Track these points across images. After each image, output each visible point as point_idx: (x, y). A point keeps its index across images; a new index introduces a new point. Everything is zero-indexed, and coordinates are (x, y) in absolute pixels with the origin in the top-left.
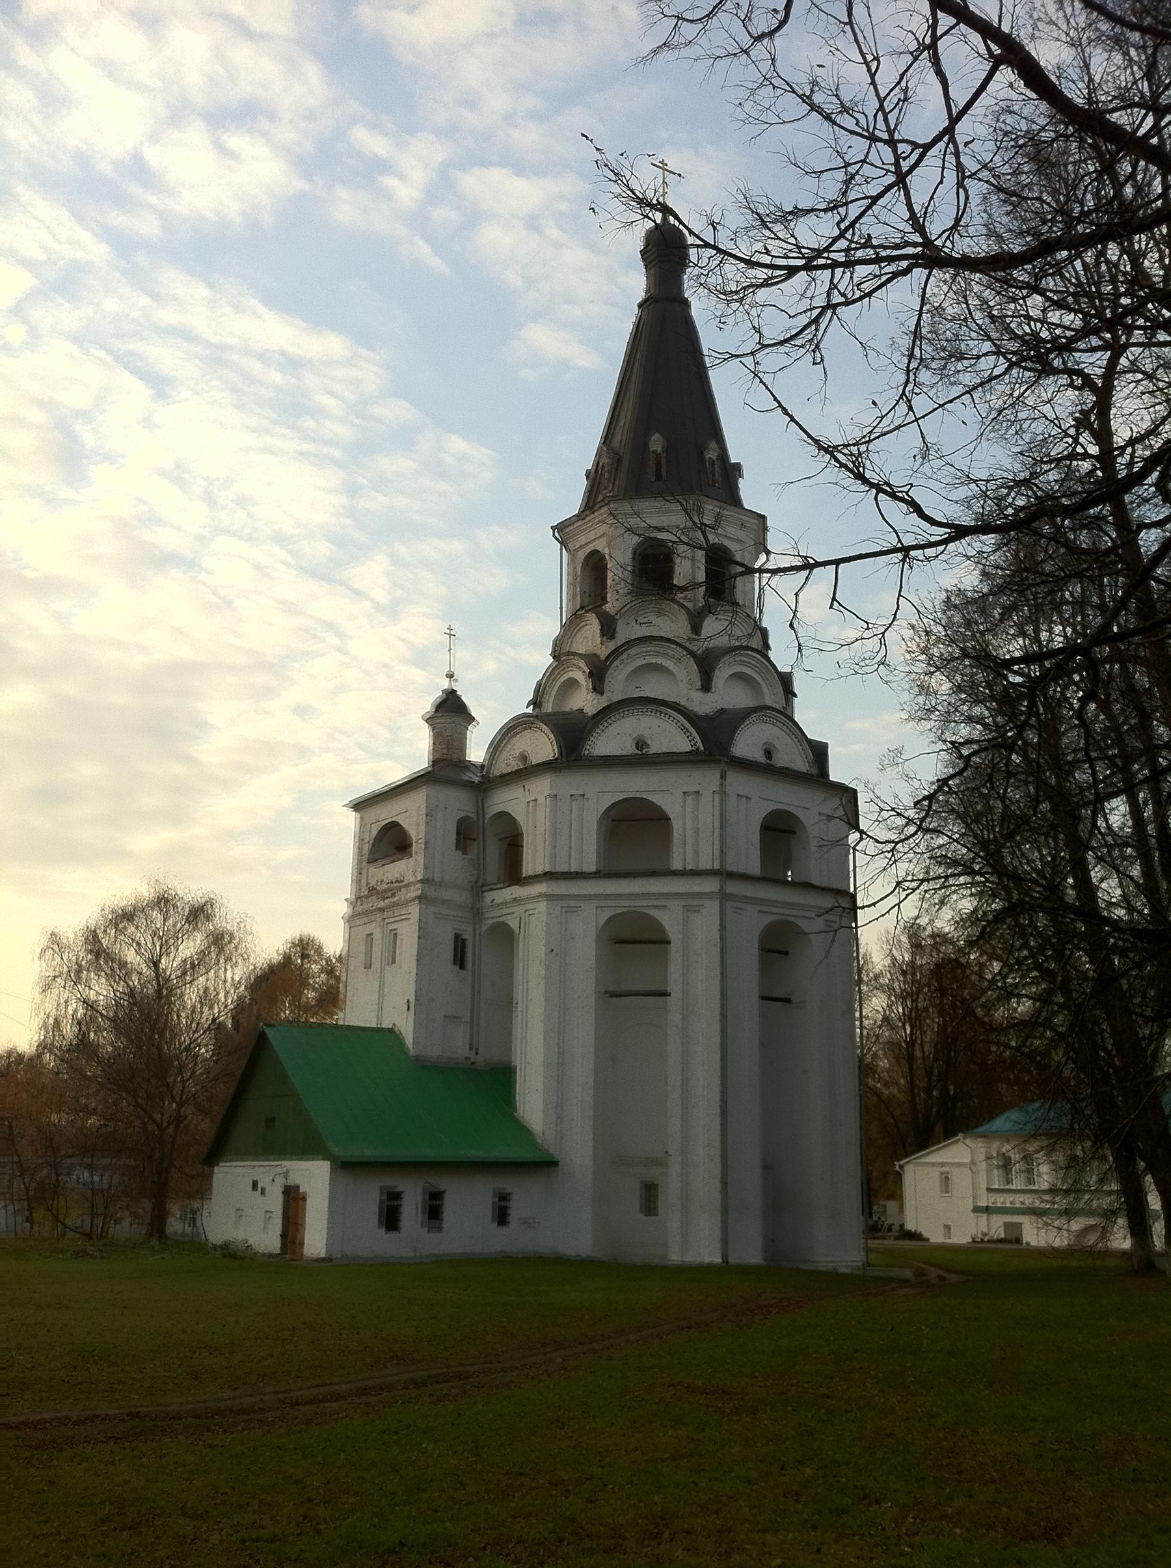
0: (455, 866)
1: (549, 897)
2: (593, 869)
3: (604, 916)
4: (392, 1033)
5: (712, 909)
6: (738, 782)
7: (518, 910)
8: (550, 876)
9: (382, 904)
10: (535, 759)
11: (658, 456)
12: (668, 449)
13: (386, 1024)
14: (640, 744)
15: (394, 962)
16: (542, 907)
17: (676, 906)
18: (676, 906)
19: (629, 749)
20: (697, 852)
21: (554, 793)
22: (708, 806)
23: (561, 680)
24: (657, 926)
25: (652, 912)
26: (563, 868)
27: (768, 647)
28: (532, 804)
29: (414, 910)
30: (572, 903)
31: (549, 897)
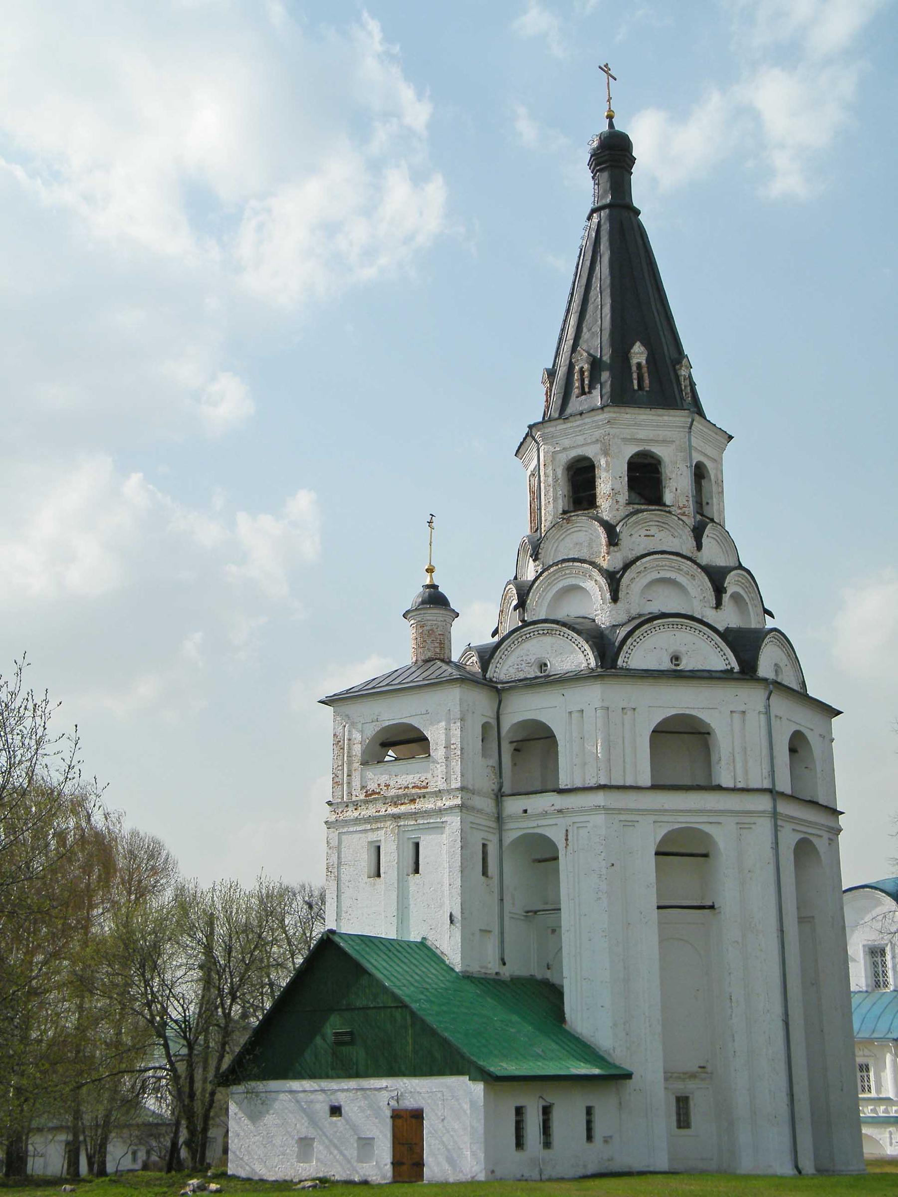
2: (649, 784)
5: (764, 826)
6: (780, 705)
7: (563, 822)
9: (393, 810)
11: (639, 365)
12: (651, 359)
14: (676, 658)
15: (417, 871)
17: (730, 823)
18: (730, 823)
19: (666, 665)
20: (746, 772)
21: (606, 704)
22: (756, 724)
25: (706, 828)
30: (629, 818)
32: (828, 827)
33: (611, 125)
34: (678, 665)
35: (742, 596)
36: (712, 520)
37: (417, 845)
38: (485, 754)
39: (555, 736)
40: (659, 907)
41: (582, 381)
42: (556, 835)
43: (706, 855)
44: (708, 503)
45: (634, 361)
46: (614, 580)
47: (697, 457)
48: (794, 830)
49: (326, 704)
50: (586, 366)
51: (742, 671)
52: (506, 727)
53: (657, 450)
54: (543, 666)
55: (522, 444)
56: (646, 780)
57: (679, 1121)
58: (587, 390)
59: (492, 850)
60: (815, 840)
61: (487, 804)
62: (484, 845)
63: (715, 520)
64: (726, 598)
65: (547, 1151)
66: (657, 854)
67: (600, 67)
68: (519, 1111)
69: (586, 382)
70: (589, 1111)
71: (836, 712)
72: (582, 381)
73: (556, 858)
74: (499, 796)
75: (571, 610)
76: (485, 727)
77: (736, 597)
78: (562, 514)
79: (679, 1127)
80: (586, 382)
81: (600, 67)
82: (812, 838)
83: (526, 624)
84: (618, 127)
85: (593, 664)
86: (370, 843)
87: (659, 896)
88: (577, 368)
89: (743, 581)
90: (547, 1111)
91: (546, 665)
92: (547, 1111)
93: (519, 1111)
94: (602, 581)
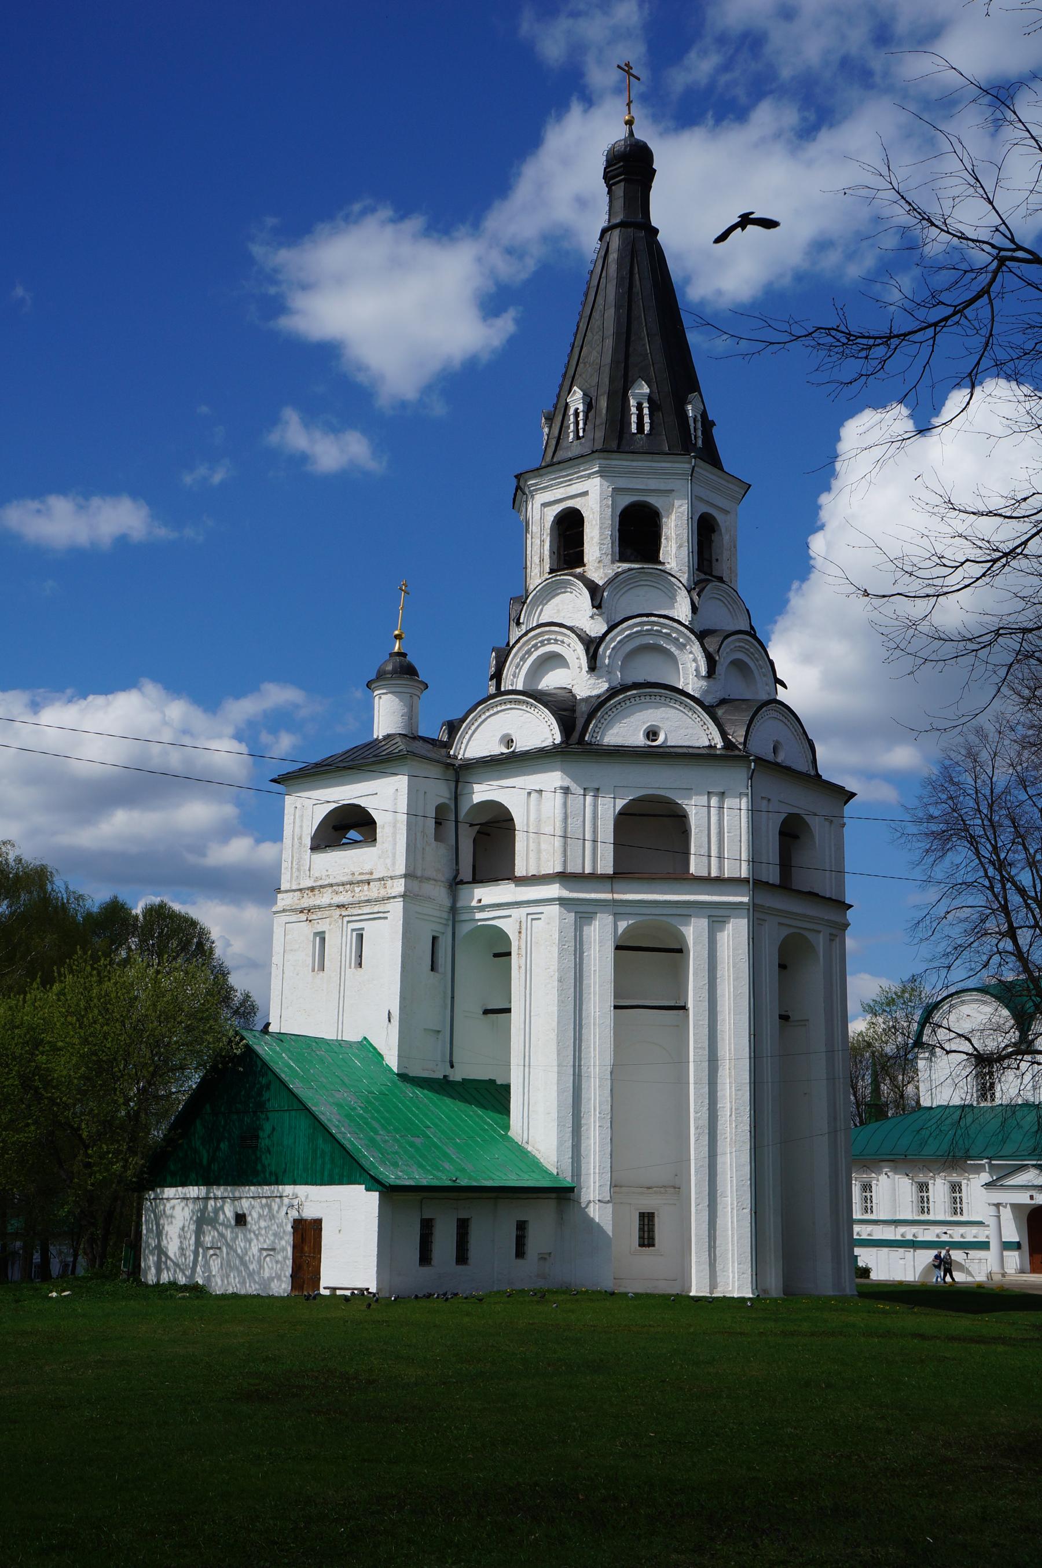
0: (436, 858)
1: (562, 902)
2: (610, 871)
3: (623, 925)
4: (365, 1046)
8: (564, 877)
10: (524, 743)
13: (352, 1035)
14: (652, 734)
15: (360, 965)
16: (555, 909)
19: (639, 739)
21: (565, 784)
23: (535, 655)
24: (681, 938)
26: (574, 868)
27: (752, 628)
28: (534, 795)
29: (396, 909)
31: (562, 902)
32: (828, 921)
33: (631, 133)
34: (656, 740)
35: (746, 664)
36: (720, 579)
37: (360, 937)
38: (438, 837)
39: (513, 820)
40: (616, 1007)
41: (577, 423)
42: (508, 926)
43: (680, 951)
44: (717, 560)
45: (633, 402)
46: (592, 646)
47: (704, 508)
48: (779, 923)
49: (279, 783)
50: (581, 407)
51: (728, 745)
52: (464, 810)
53: (653, 500)
54: (509, 742)
55: (515, 495)
56: (606, 865)
57: (641, 1238)
58: (581, 434)
59: (445, 943)
60: (809, 936)
61: (440, 893)
62: (434, 939)
63: (724, 579)
64: (720, 669)
65: (461, 1267)
66: (618, 948)
67: (619, 67)
68: (427, 1228)
69: (581, 425)
70: (522, 1226)
71: (849, 794)
72: (577, 423)
73: (509, 954)
74: (455, 884)
75: (552, 681)
76: (440, 810)
77: (739, 665)
78: (550, 573)
79: (642, 1245)
80: (581, 425)
81: (619, 67)
82: (806, 934)
83: (499, 693)
84: (638, 135)
85: (558, 740)
86: (316, 934)
87: (617, 996)
88: (572, 411)
89: (747, 647)
90: (463, 1227)
91: (512, 741)
92: (463, 1227)
93: (427, 1228)
94: (580, 649)
